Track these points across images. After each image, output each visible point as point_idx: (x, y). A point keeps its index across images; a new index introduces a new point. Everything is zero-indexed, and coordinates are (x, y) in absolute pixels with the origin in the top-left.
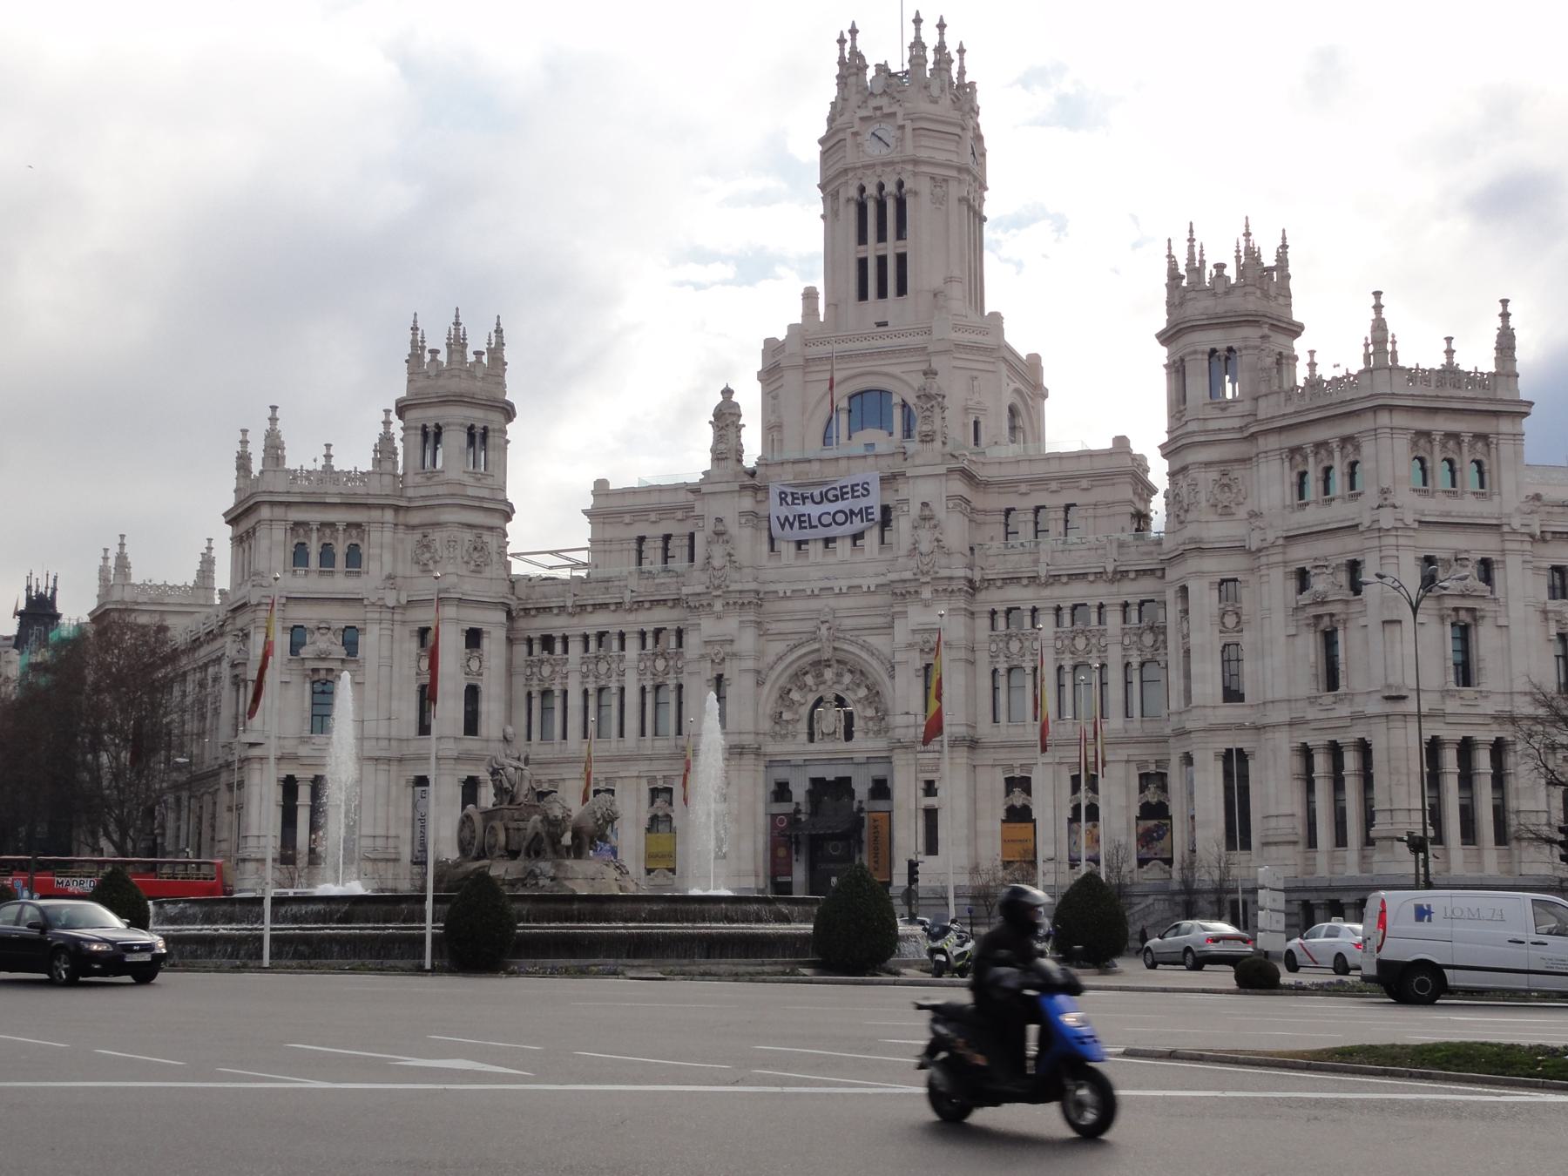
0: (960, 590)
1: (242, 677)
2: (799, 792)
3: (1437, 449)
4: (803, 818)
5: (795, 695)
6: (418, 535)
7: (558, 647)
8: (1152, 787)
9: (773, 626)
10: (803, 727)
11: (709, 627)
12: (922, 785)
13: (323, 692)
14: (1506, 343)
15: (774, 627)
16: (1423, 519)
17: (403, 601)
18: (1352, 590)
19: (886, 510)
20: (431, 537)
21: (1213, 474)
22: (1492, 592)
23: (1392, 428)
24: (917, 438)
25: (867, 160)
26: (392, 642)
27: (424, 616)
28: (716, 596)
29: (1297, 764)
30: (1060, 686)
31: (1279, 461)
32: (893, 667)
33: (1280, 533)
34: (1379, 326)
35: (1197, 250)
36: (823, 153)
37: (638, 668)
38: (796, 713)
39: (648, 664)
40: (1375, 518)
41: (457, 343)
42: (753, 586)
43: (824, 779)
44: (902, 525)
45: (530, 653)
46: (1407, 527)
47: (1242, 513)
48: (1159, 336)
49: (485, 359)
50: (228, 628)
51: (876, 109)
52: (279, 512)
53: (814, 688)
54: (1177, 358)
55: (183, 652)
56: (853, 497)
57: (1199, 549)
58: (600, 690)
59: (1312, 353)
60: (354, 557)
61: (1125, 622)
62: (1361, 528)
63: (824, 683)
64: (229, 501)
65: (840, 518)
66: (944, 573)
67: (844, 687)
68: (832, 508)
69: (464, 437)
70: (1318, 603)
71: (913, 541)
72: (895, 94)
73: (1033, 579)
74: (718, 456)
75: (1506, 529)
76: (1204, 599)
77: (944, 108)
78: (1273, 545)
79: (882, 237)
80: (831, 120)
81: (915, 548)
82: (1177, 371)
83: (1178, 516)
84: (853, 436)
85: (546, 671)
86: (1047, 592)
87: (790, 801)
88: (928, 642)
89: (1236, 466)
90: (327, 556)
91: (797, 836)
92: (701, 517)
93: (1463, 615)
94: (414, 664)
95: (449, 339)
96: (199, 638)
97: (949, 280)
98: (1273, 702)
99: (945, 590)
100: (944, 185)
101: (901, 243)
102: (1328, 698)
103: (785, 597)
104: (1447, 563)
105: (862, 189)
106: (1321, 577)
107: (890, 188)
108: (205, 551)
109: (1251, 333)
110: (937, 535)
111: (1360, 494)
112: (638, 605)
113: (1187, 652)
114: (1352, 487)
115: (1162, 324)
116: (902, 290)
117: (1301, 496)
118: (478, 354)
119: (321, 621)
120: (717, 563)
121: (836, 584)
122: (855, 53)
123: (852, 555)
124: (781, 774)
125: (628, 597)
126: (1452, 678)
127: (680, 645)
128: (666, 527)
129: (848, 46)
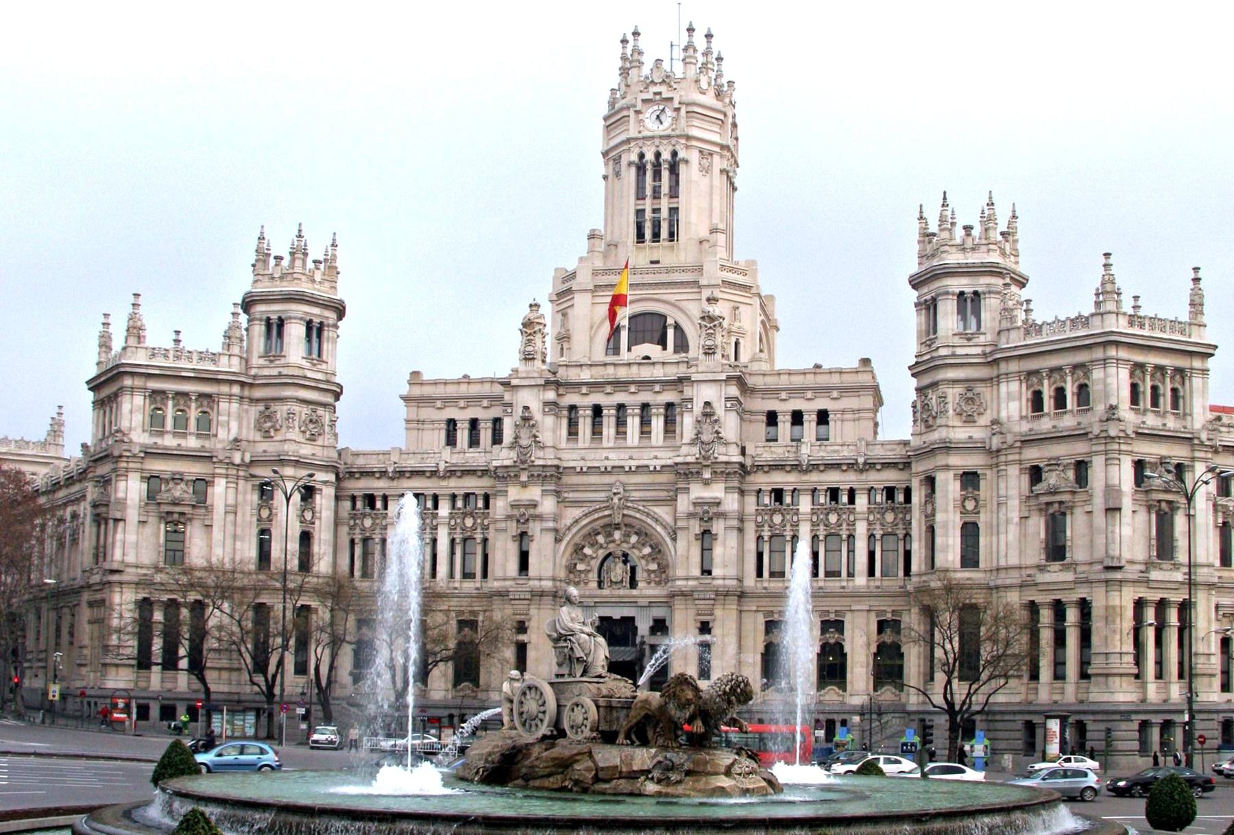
0: (735, 472)
1: (104, 515)
7: (379, 504)
9: (571, 495)
13: (175, 531)
15: (572, 496)
16: (1140, 431)
18: (1077, 483)
21: (959, 389)
23: (1117, 360)
25: (646, 133)
26: (237, 493)
28: (523, 469)
31: (1018, 382)
33: (1018, 438)
37: (449, 524)
38: (589, 565)
39: (458, 521)
40: (1105, 428)
42: (556, 462)
45: (354, 507)
46: (1127, 436)
47: (984, 420)
50: (90, 475)
53: (605, 545)
55: (44, 493)
57: (947, 447)
61: (869, 503)
62: (1090, 436)
63: (613, 541)
66: (722, 458)
67: (630, 545)
70: (1051, 493)
71: (695, 431)
72: (672, 84)
75: (1196, 442)
77: (709, 99)
78: (1011, 447)
80: (612, 104)
81: (697, 438)
85: (368, 523)
88: (708, 512)
89: (978, 385)
92: (510, 405)
96: (59, 482)
97: (714, 230)
99: (722, 472)
100: (709, 157)
103: (581, 472)
104: (1154, 466)
106: (1054, 473)
108: (55, 416)
109: (998, 281)
110: (716, 428)
112: (451, 473)
113: (931, 530)
119: (178, 473)
121: (627, 464)
125: (442, 466)
127: (487, 506)
128: (471, 413)
129: (630, 46)
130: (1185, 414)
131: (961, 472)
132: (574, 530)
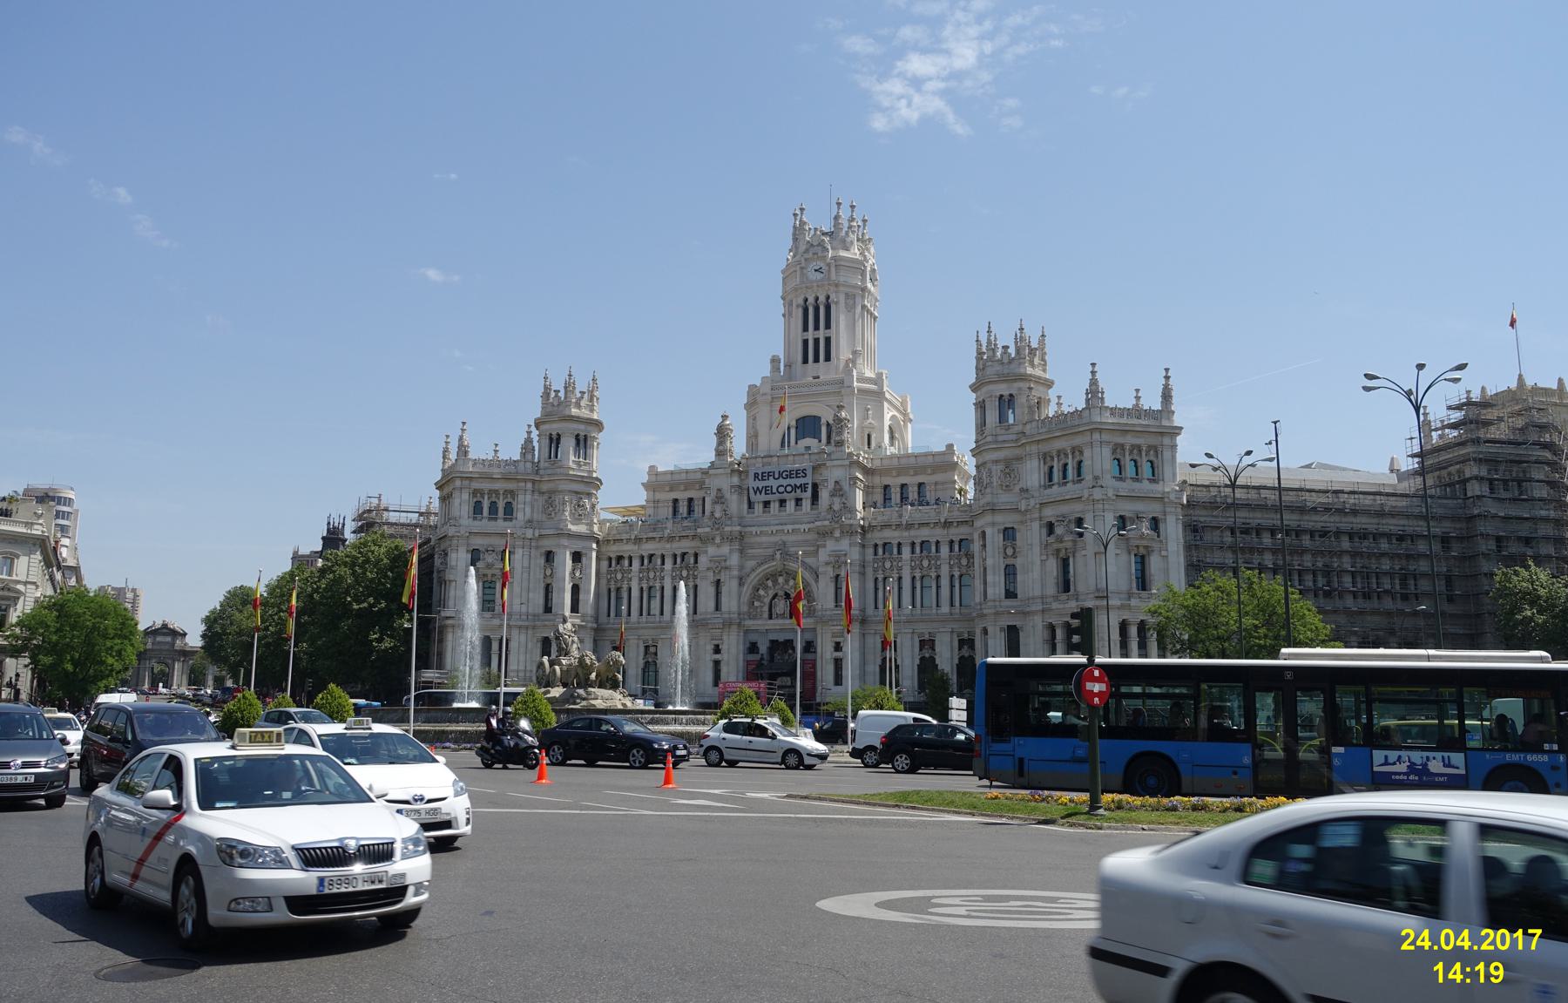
2: (763, 648)
3: (1127, 454)
4: (765, 662)
5: (762, 592)
6: (546, 497)
8: (966, 647)
9: (750, 551)
10: (766, 609)
11: (712, 550)
12: (833, 644)
14: (1167, 396)
17: (537, 535)
19: (815, 486)
20: (553, 498)
22: (1158, 536)
24: (833, 444)
27: (548, 544)
29: (1047, 635)
30: (914, 588)
32: (818, 576)
34: (1094, 382)
35: (992, 338)
36: (784, 279)
41: (569, 387)
43: (777, 641)
44: (824, 495)
46: (1109, 499)
47: (1017, 489)
48: (970, 387)
49: (586, 396)
51: (814, 254)
52: (466, 483)
54: (981, 400)
56: (797, 477)
58: (650, 588)
59: (1059, 397)
60: (509, 511)
61: (951, 551)
62: (1083, 499)
64: (438, 477)
65: (789, 489)
68: (785, 482)
69: (573, 442)
73: (898, 526)
74: (720, 453)
75: (1166, 500)
76: (995, 539)
79: (817, 328)
82: (981, 407)
83: (981, 491)
84: (799, 442)
86: (906, 534)
87: (758, 653)
90: (493, 508)
91: (761, 674)
93: (1142, 551)
94: (543, 571)
95: (566, 384)
98: (1033, 598)
101: (828, 331)
102: (1064, 596)
105: (806, 300)
107: (822, 299)
111: (1083, 480)
112: (671, 539)
113: (985, 569)
114: (1079, 475)
115: (973, 380)
116: (828, 358)
117: (1051, 479)
118: (583, 393)
120: (717, 515)
122: (803, 223)
123: (795, 511)
124: (753, 637)
126: (1134, 585)
127: (696, 562)
130: (1159, 480)
131: (1003, 527)
132: (752, 576)
